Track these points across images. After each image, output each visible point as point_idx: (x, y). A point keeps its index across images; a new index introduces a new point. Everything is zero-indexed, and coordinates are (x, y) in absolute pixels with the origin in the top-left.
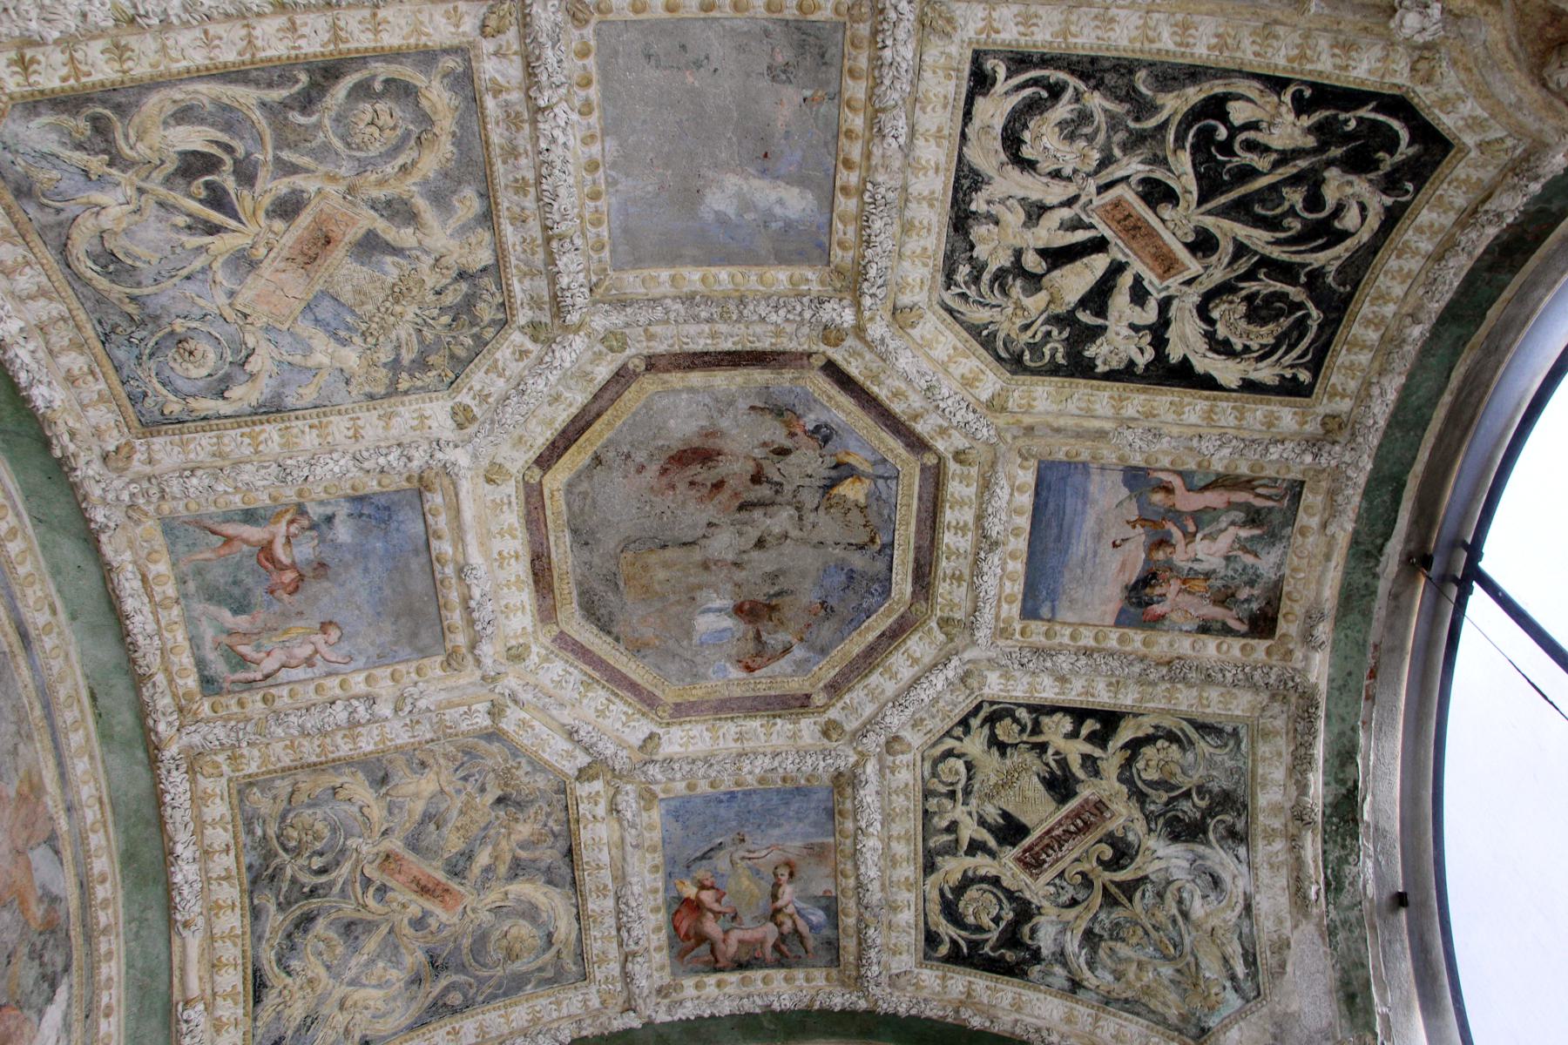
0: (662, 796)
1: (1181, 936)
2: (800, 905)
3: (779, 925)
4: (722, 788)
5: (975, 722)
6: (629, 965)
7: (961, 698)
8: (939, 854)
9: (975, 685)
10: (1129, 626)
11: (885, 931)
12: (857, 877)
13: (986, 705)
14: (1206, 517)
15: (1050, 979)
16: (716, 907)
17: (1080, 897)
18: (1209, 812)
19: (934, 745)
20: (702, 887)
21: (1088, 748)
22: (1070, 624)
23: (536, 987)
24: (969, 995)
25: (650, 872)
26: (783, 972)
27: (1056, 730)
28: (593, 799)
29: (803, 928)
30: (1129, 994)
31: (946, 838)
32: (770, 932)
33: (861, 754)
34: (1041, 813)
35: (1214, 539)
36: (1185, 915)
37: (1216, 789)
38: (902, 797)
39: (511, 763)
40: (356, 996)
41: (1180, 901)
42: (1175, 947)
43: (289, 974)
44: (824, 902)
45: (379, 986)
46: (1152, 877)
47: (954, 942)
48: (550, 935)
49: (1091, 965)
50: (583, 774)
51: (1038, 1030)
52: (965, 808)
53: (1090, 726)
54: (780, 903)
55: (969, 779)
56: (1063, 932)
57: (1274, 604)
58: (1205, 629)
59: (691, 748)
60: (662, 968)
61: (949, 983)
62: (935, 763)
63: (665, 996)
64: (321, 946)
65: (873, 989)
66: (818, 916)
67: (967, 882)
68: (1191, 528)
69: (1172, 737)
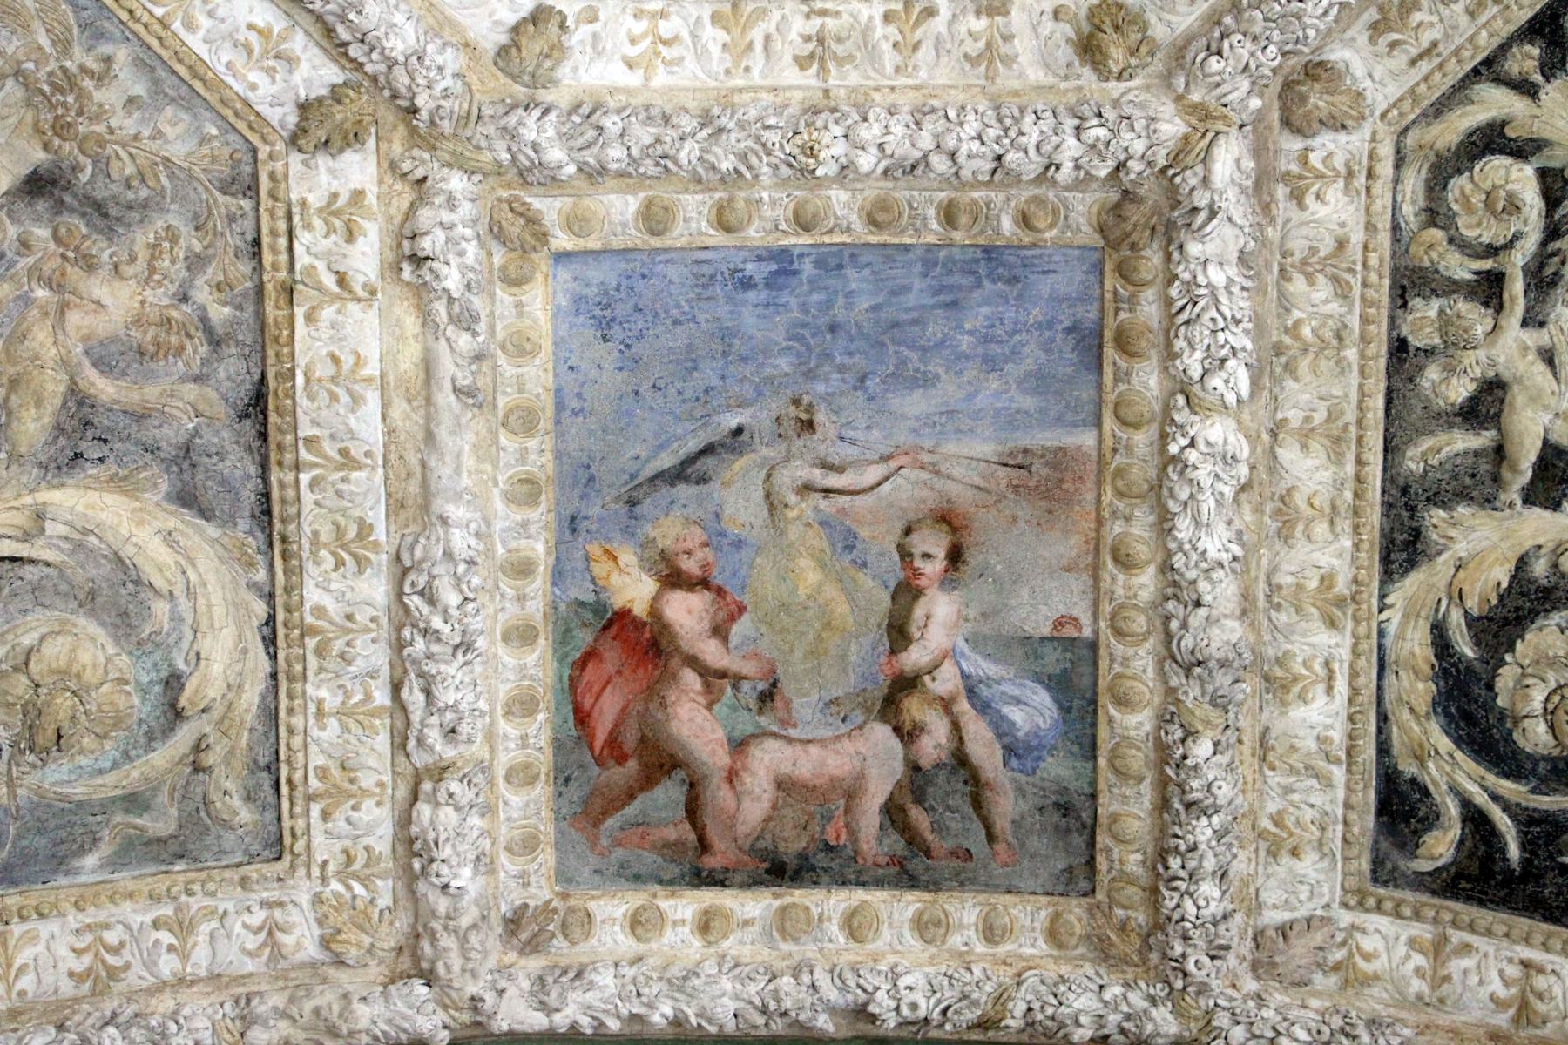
0: (562, 240)
2: (981, 666)
3: (908, 735)
4: (754, 234)
6: (424, 810)
8: (1437, 498)
11: (1247, 770)
12: (1167, 568)
16: (712, 653)
19: (1440, 108)
20: (673, 579)
23: (115, 863)
24: (1524, 1012)
25: (510, 499)
26: (910, 903)
28: (343, 216)
29: (983, 748)
32: (876, 757)
33: (1202, 113)
39: (79, 56)
44: (1053, 659)
47: (1475, 819)
48: (174, 682)
50: (318, 128)
52: (1532, 338)
54: (914, 657)
59: (661, 79)
60: (529, 845)
61: (1457, 966)
62: (1437, 182)
63: (532, 947)
65: (1196, 961)
66: (1033, 710)
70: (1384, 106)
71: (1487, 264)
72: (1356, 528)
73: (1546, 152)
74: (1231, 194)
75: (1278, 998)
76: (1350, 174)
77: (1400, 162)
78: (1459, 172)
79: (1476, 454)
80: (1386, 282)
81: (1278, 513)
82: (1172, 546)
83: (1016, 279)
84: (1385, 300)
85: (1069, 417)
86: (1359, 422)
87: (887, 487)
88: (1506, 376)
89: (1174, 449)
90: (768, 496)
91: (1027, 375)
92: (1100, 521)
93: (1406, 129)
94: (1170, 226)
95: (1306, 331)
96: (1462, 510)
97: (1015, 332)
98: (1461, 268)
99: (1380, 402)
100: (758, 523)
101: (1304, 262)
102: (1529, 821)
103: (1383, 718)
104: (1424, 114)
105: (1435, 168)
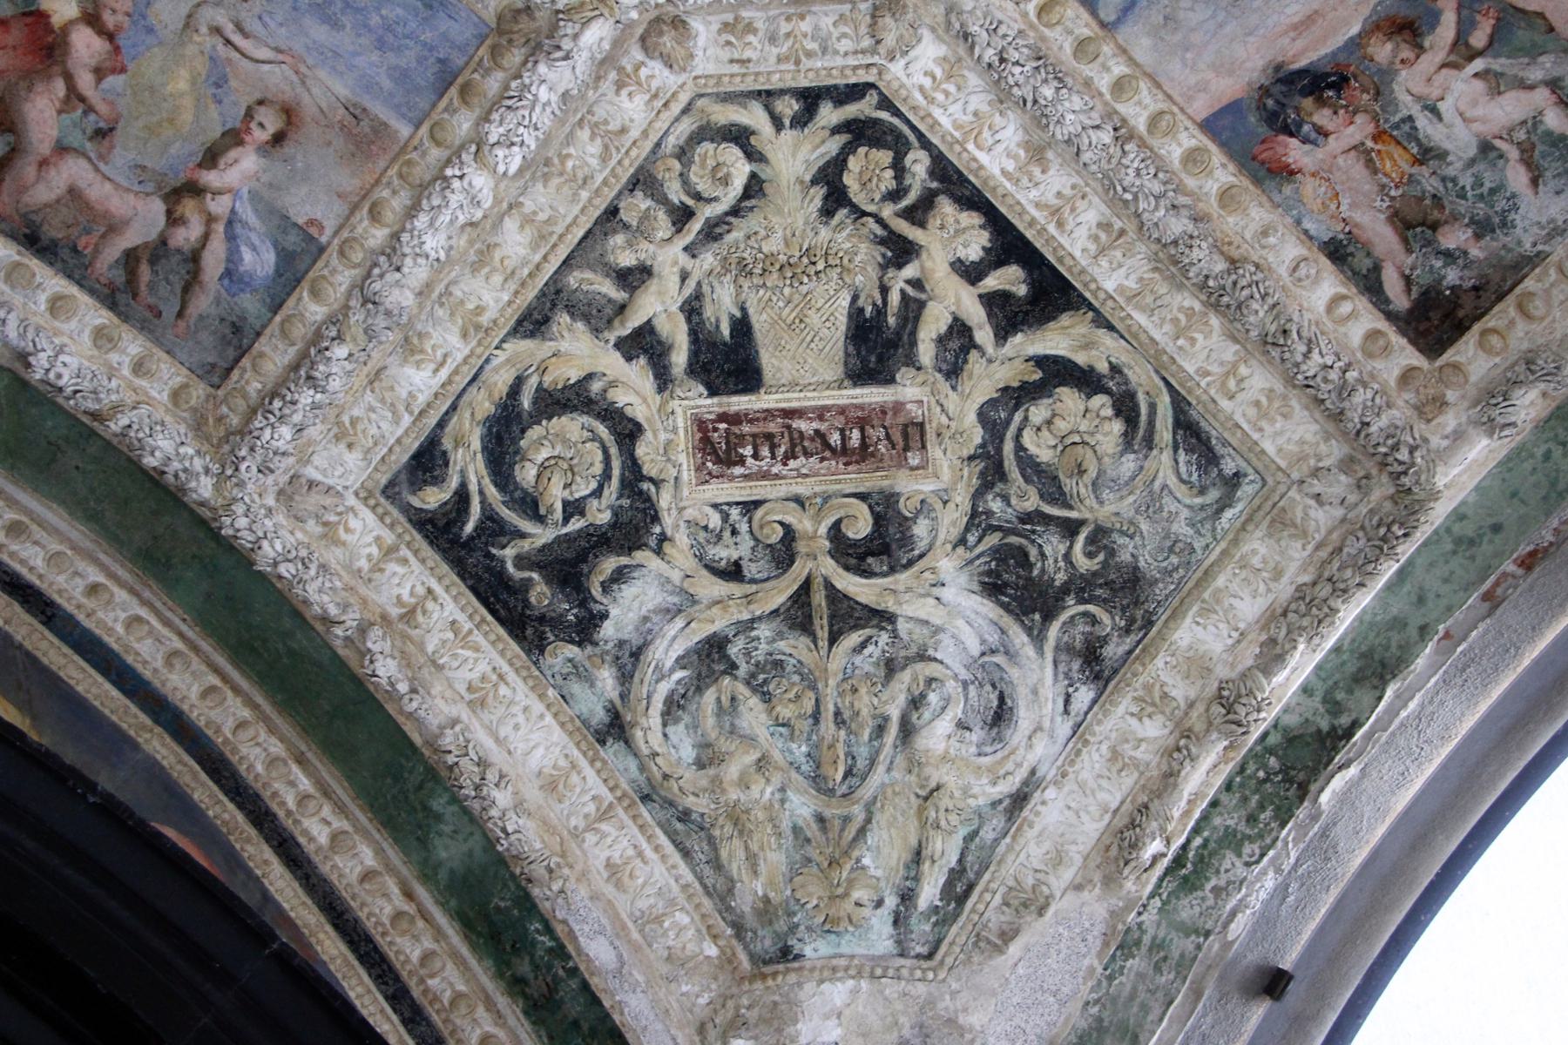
1: (873, 762)
2: (246, 212)
3: (174, 220)
5: (829, 115)
7: (846, 45)
8: (571, 309)
9: (890, 40)
10: (1223, 145)
11: (359, 380)
12: (396, 236)
13: (872, 98)
14: (1522, 35)
15: (576, 688)
16: (85, 81)
17: (750, 570)
18: (1082, 587)
20: (92, 19)
21: (975, 314)
22: (1131, 61)
24: (409, 615)
26: (102, 317)
27: (954, 237)
29: (214, 261)
30: (699, 805)
31: (609, 289)
32: (144, 218)
34: (804, 369)
35: (1496, 92)
36: (907, 731)
37: (1125, 557)
38: (594, 148)
41: (916, 702)
42: (848, 773)
44: (292, 240)
46: (902, 626)
47: (462, 497)
49: (674, 707)
51: (483, 763)
52: (684, 259)
53: (1010, 279)
54: (211, 178)
55: (735, 211)
56: (671, 613)
57: (1488, 296)
58: (1337, 252)
61: (393, 567)
62: (697, 137)
65: (249, 469)
66: (259, 260)
67: (575, 398)
68: (1479, 39)
69: (1126, 407)
70: (698, 72)
71: (690, 202)
72: (516, 293)
73: (763, 165)
74: (585, 54)
75: (280, 518)
76: (655, 96)
77: (686, 110)
78: (712, 141)
79: (610, 300)
80: (632, 170)
81: (481, 252)
82: (408, 226)
83: (431, 7)
84: (624, 180)
85: (404, 110)
86: (561, 236)
87: (266, 67)
88: (656, 269)
89: (449, 172)
90: (189, 16)
91: (396, 68)
92: (378, 182)
93: (702, 95)
94: (539, 46)
95: (570, 164)
96: (580, 325)
97: (407, 37)
98: (676, 194)
99: (581, 234)
100: (171, 27)
101: (596, 125)
102: (489, 516)
103: (454, 407)
104: (717, 95)
105: (702, 129)
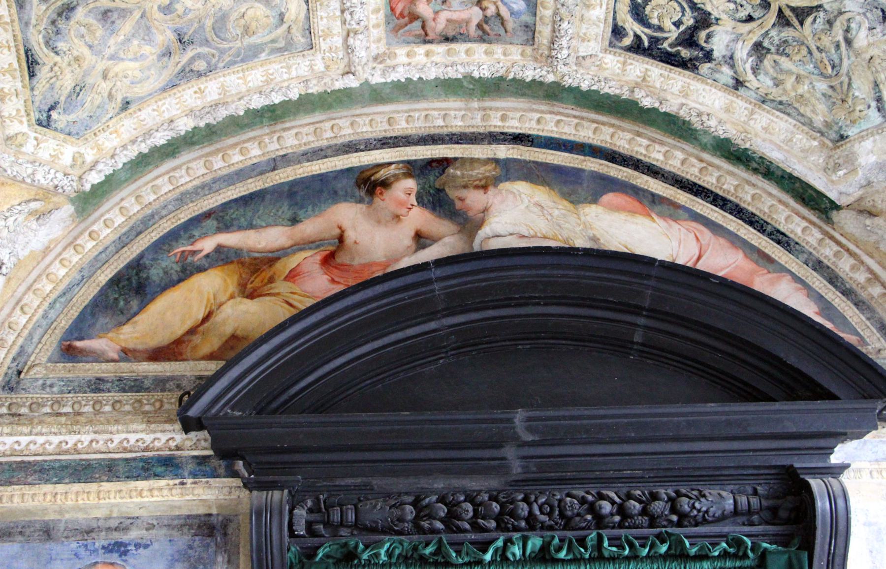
1: (841, 59)
3: (484, 9)
6: (351, 41)
11: (577, 22)
15: (717, 76)
17: (755, 15)
23: (269, 54)
24: (644, 79)
26: (484, 46)
30: (784, 99)
32: (476, 15)
36: (849, 42)
40: (117, 69)
41: (847, 30)
42: (833, 67)
43: (57, 53)
45: (135, 59)
46: (826, 7)
47: (637, 37)
48: (282, 16)
49: (755, 70)
51: (699, 115)
56: (736, 40)
60: (379, 40)
61: (628, 68)
63: (381, 63)
64: (83, 30)
75: (582, 71)
102: (651, 38)
103: (615, 12)
